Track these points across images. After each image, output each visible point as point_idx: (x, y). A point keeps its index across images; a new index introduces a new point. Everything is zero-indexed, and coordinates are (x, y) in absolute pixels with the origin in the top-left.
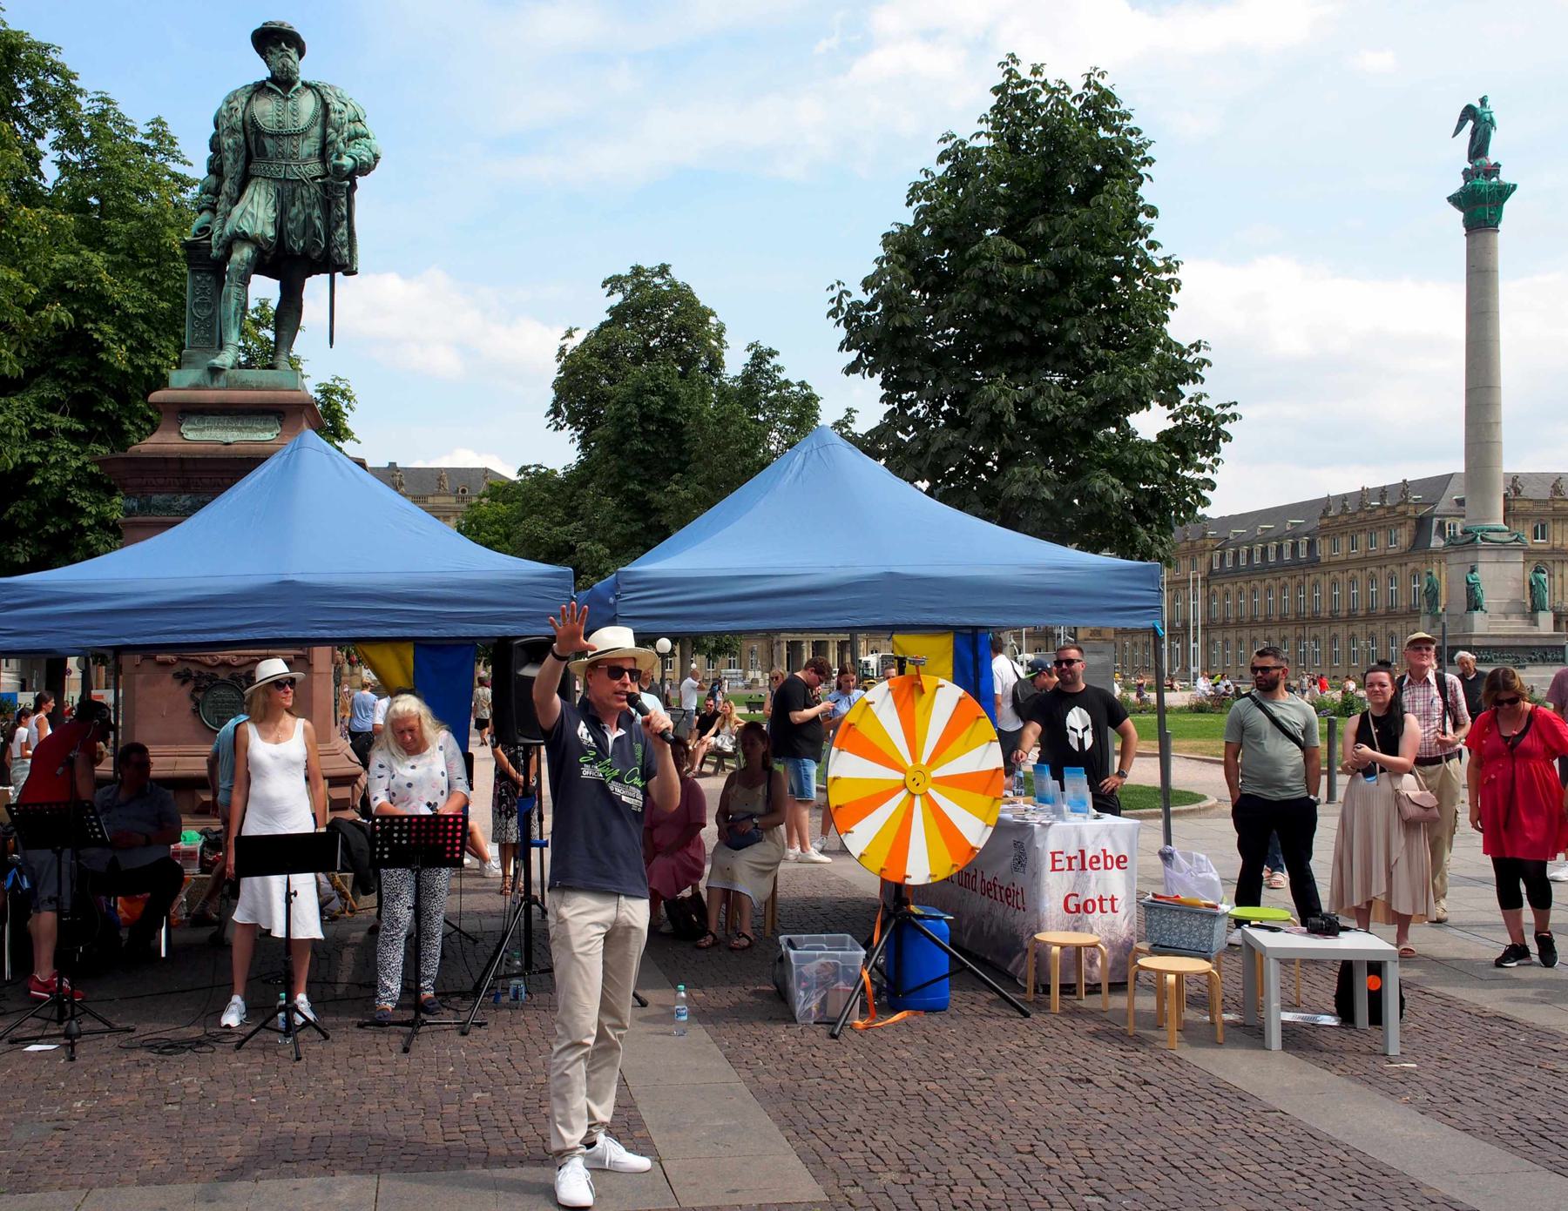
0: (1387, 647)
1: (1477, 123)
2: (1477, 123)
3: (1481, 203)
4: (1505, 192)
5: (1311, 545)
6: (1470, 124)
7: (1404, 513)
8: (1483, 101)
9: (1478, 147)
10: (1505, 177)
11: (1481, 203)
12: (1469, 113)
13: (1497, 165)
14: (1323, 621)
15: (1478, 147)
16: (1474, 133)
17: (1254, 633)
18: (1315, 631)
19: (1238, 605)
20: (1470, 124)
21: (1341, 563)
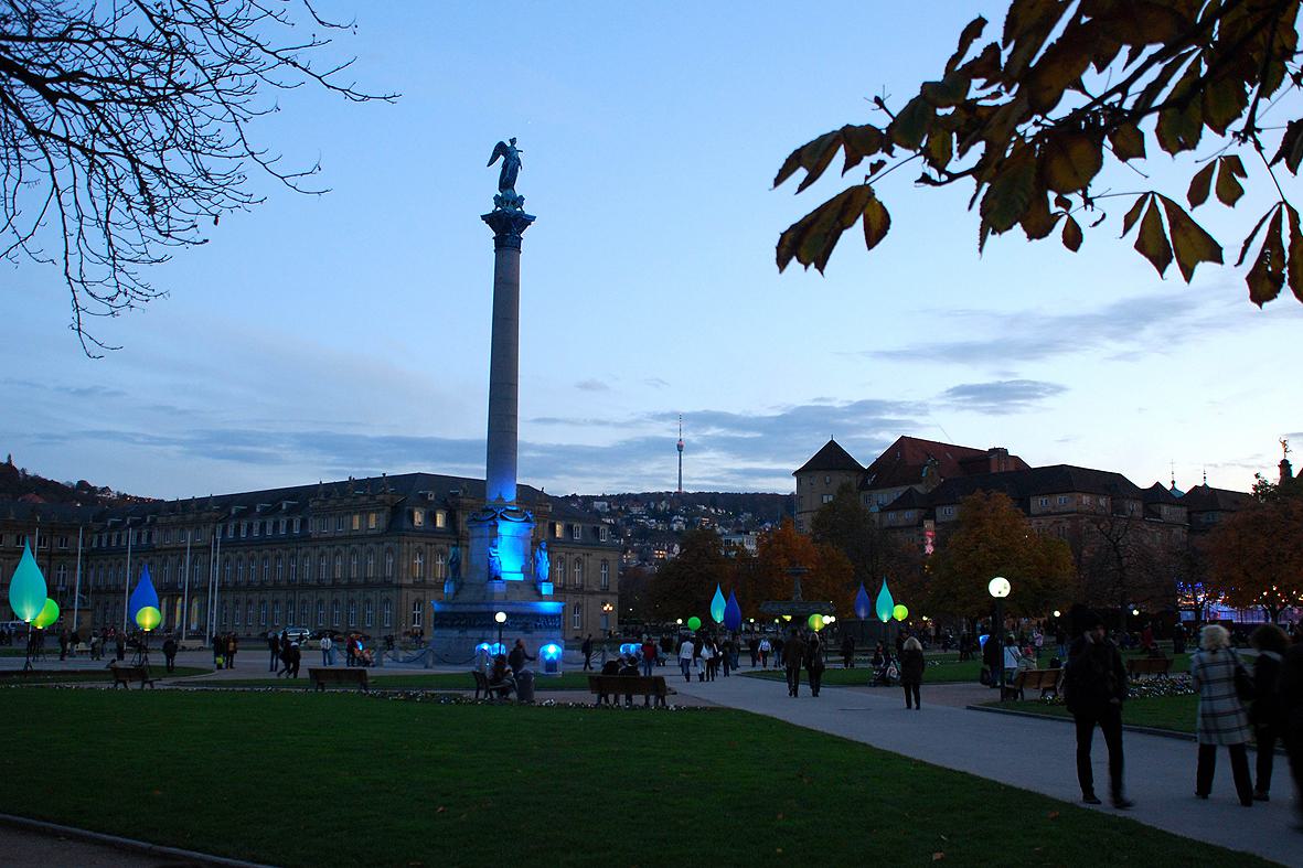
0: (364, 611)
1: (507, 157)
2: (507, 157)
3: (508, 224)
4: (526, 221)
5: (304, 524)
6: (502, 159)
7: (383, 501)
8: (513, 141)
9: (508, 180)
10: (527, 209)
11: (508, 224)
12: (501, 149)
13: (522, 198)
14: (311, 587)
15: (508, 180)
16: (505, 166)
17: (250, 596)
18: (304, 596)
19: (236, 571)
20: (502, 159)
21: (328, 539)
